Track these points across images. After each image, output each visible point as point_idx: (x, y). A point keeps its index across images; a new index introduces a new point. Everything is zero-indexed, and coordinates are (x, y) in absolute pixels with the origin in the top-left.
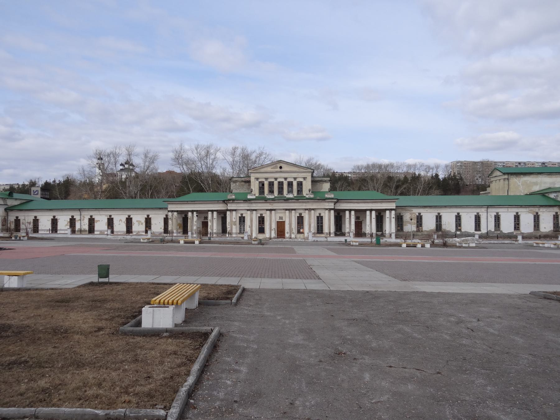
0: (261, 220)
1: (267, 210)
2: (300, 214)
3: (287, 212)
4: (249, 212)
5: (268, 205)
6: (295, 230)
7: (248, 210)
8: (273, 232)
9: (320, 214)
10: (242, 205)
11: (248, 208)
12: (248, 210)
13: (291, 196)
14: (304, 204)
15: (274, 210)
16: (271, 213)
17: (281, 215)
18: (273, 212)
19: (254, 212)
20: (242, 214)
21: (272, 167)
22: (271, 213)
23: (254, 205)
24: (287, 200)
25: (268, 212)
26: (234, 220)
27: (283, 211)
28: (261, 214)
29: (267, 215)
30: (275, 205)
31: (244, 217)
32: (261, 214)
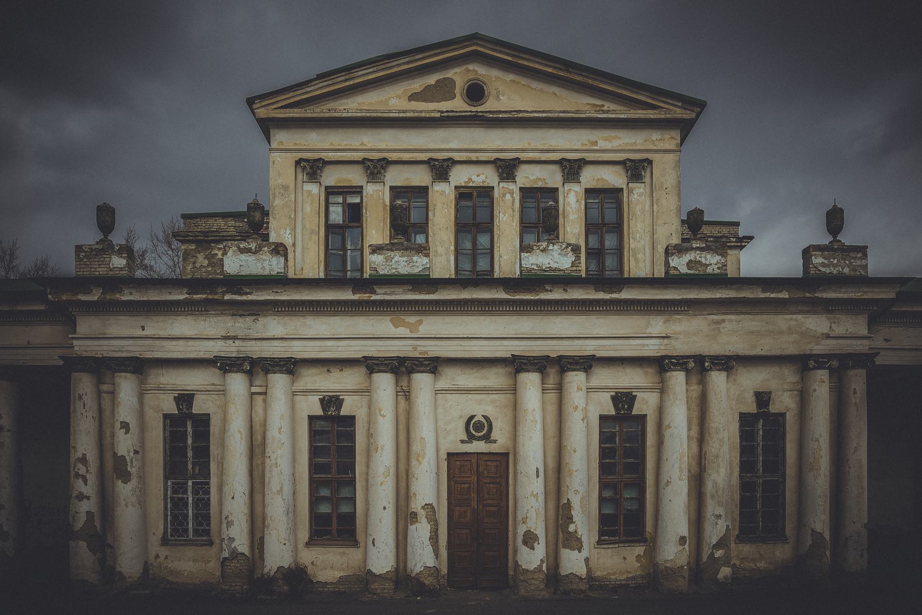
0: (333, 441)
1: (372, 365)
2: (624, 399)
3: (530, 382)
4: (237, 383)
5: (382, 325)
6: (584, 524)
7: (226, 365)
8: (421, 532)
9: (763, 398)
10: (183, 326)
11: (230, 349)
12: (226, 365)
13: (555, 258)
14: (657, 325)
15: (434, 365)
16: (405, 394)
17: (481, 407)
18: (422, 381)
19: (279, 382)
20: (185, 399)
21: (417, 85)
22: (405, 394)
23: (274, 326)
24: (529, 292)
25: (384, 383)
26: (125, 444)
27: (495, 378)
28: (331, 402)
29: (376, 407)
30: (432, 325)
31: (203, 422)
32: (331, 402)
